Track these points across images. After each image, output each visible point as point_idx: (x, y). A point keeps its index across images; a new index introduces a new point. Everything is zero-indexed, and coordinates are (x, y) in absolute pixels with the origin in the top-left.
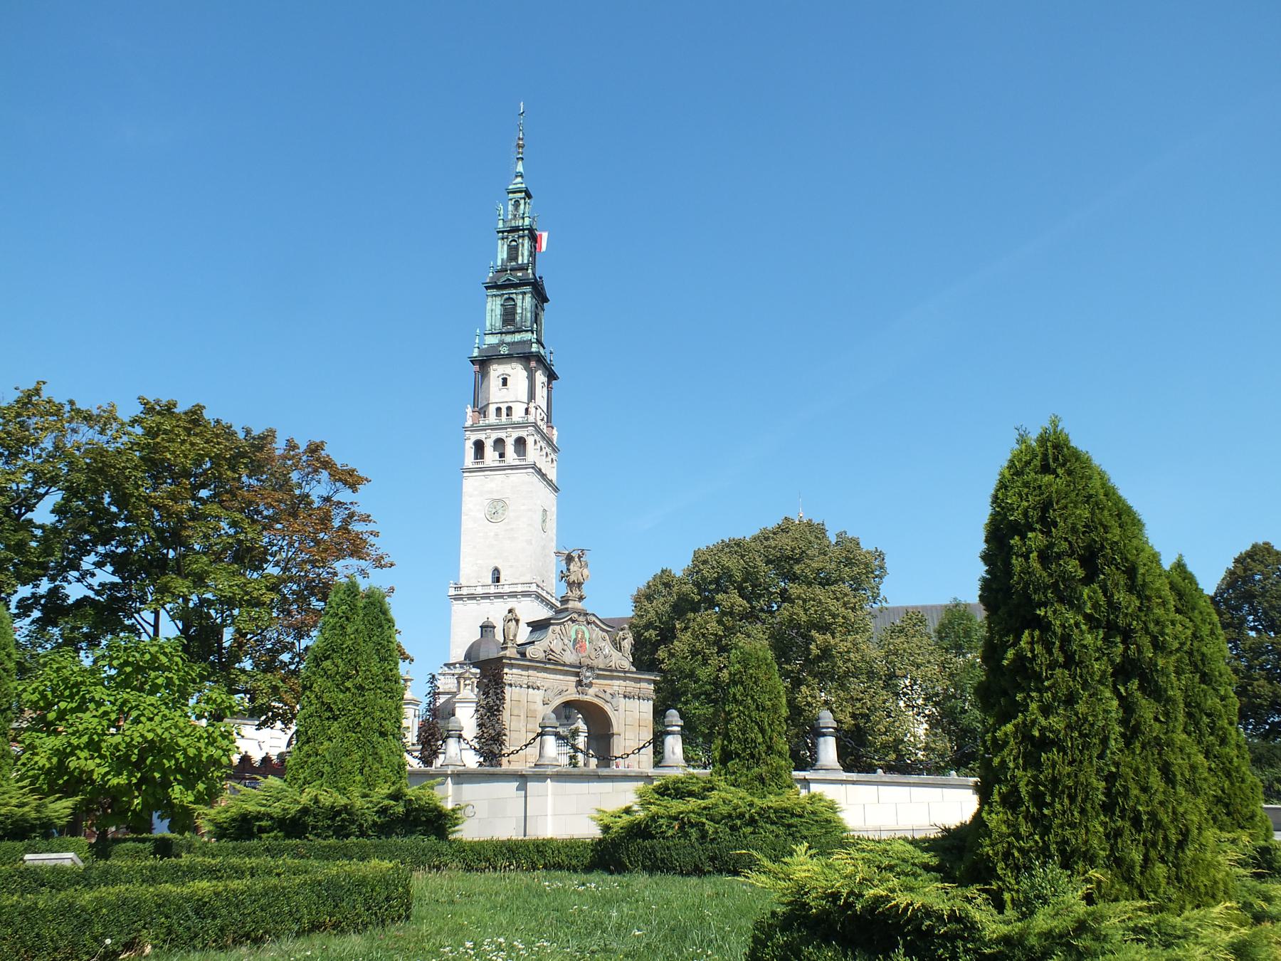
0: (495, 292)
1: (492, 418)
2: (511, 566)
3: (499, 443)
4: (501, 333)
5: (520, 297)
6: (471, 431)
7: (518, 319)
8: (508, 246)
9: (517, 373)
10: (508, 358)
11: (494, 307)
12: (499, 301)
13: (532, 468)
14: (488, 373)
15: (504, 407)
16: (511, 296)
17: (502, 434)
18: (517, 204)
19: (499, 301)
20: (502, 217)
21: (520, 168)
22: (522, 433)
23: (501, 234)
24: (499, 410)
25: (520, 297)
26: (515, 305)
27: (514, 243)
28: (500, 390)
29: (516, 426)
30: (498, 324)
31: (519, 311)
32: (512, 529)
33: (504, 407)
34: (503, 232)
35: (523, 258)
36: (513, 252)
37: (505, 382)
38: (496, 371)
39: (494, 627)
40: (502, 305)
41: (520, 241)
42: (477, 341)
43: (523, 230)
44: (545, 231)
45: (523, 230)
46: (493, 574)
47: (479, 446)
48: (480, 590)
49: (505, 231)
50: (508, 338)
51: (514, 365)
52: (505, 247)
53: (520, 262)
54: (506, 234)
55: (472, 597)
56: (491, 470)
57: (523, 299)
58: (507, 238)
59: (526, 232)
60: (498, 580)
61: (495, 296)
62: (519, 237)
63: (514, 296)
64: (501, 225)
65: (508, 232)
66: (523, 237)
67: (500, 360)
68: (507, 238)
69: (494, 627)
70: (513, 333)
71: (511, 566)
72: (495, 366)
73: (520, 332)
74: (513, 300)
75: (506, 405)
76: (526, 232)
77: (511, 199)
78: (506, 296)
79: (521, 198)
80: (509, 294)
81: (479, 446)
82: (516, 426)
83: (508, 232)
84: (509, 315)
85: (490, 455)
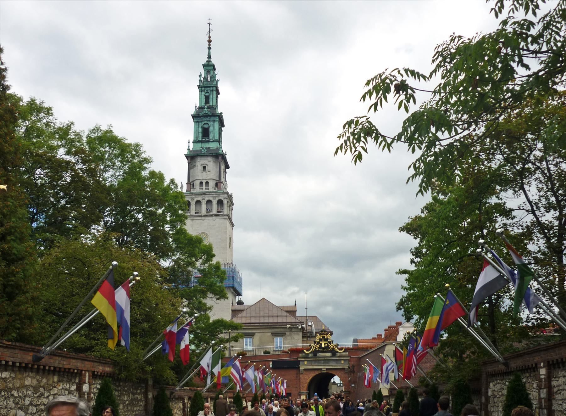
1: (197, 189)
4: (202, 142)
15: (204, 182)
22: (221, 198)
24: (201, 183)
26: (209, 127)
28: (202, 172)
33: (204, 182)
37: (204, 168)
50: (206, 145)
53: (211, 104)
54: (203, 89)
58: (204, 91)
63: (208, 122)
68: (204, 91)
72: (199, 159)
76: (215, 88)
83: (205, 87)
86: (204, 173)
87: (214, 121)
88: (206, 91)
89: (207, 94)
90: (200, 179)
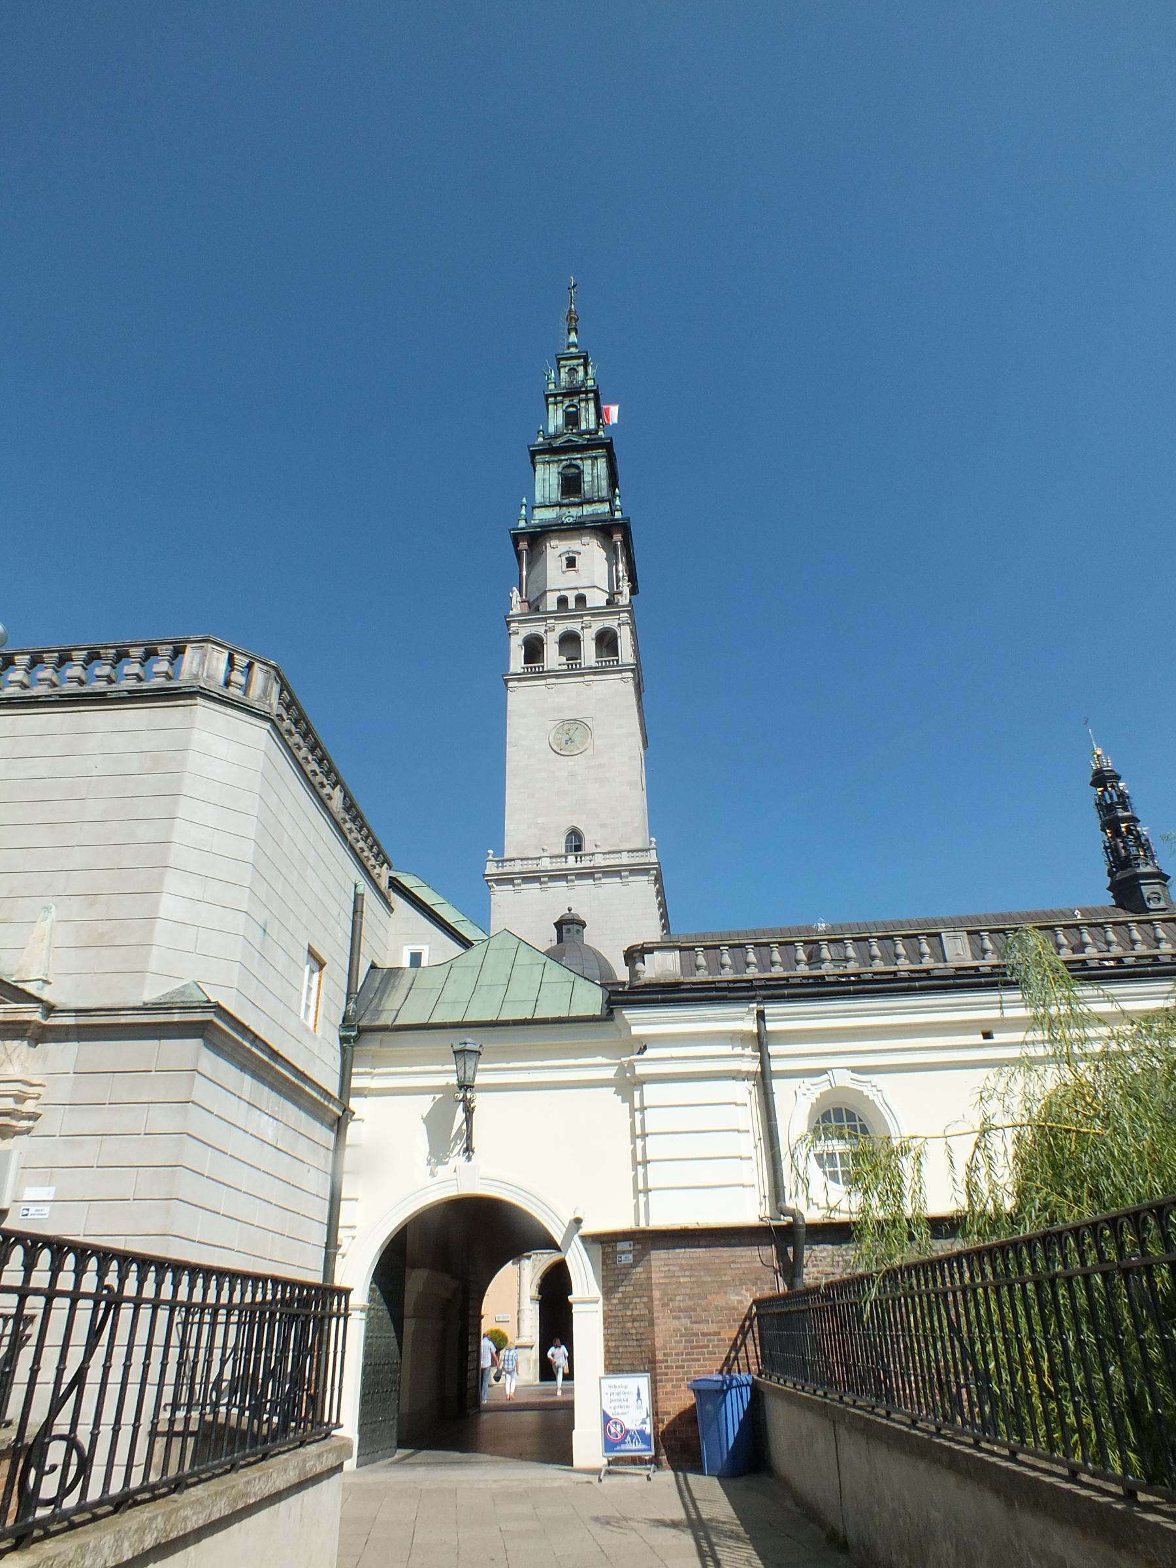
0: (547, 458)
2: (603, 826)
3: (570, 641)
4: (561, 505)
5: (589, 462)
6: (520, 622)
7: (586, 487)
8: (564, 411)
9: (592, 552)
10: (577, 528)
11: (547, 476)
12: (554, 469)
13: (632, 670)
14: (542, 553)
15: (571, 597)
16: (574, 462)
17: (574, 626)
18: (573, 370)
19: (554, 469)
20: (553, 381)
21: (573, 338)
23: (551, 400)
24: (563, 601)
25: (589, 462)
27: (571, 409)
28: (563, 572)
29: (597, 613)
30: (556, 495)
31: (587, 478)
32: (601, 766)
33: (571, 597)
34: (555, 396)
35: (588, 420)
36: (572, 419)
37: (571, 563)
38: (555, 550)
39: (583, 924)
40: (559, 473)
41: (583, 404)
42: (523, 512)
43: (587, 392)
44: (614, 403)
45: (587, 392)
46: (568, 840)
47: (534, 649)
48: (546, 864)
49: (559, 395)
50: (575, 512)
51: (585, 539)
52: (560, 412)
53: (583, 426)
54: (559, 398)
55: (532, 878)
56: (557, 677)
57: (593, 465)
58: (562, 402)
59: (591, 395)
60: (578, 848)
61: (548, 462)
62: (580, 401)
63: (579, 462)
64: (552, 386)
65: (564, 395)
66: (587, 400)
67: (563, 534)
68: (562, 402)
69: (583, 924)
70: (580, 504)
71: (603, 826)
72: (554, 543)
73: (590, 502)
74: (577, 467)
75: (576, 592)
76: (591, 395)
77: (565, 367)
78: (568, 462)
79: (578, 365)
80: (570, 459)
81: (534, 649)
82: (597, 613)
83: (564, 395)
84: (571, 484)
85: (553, 657)
86: (571, 573)
87: (596, 458)
88: (567, 403)
89: (571, 409)
90: (559, 590)
